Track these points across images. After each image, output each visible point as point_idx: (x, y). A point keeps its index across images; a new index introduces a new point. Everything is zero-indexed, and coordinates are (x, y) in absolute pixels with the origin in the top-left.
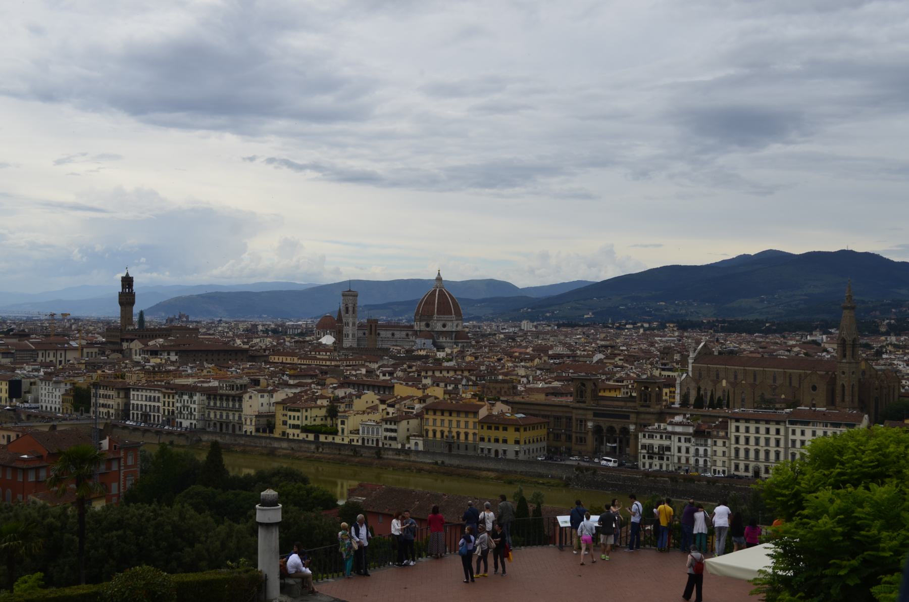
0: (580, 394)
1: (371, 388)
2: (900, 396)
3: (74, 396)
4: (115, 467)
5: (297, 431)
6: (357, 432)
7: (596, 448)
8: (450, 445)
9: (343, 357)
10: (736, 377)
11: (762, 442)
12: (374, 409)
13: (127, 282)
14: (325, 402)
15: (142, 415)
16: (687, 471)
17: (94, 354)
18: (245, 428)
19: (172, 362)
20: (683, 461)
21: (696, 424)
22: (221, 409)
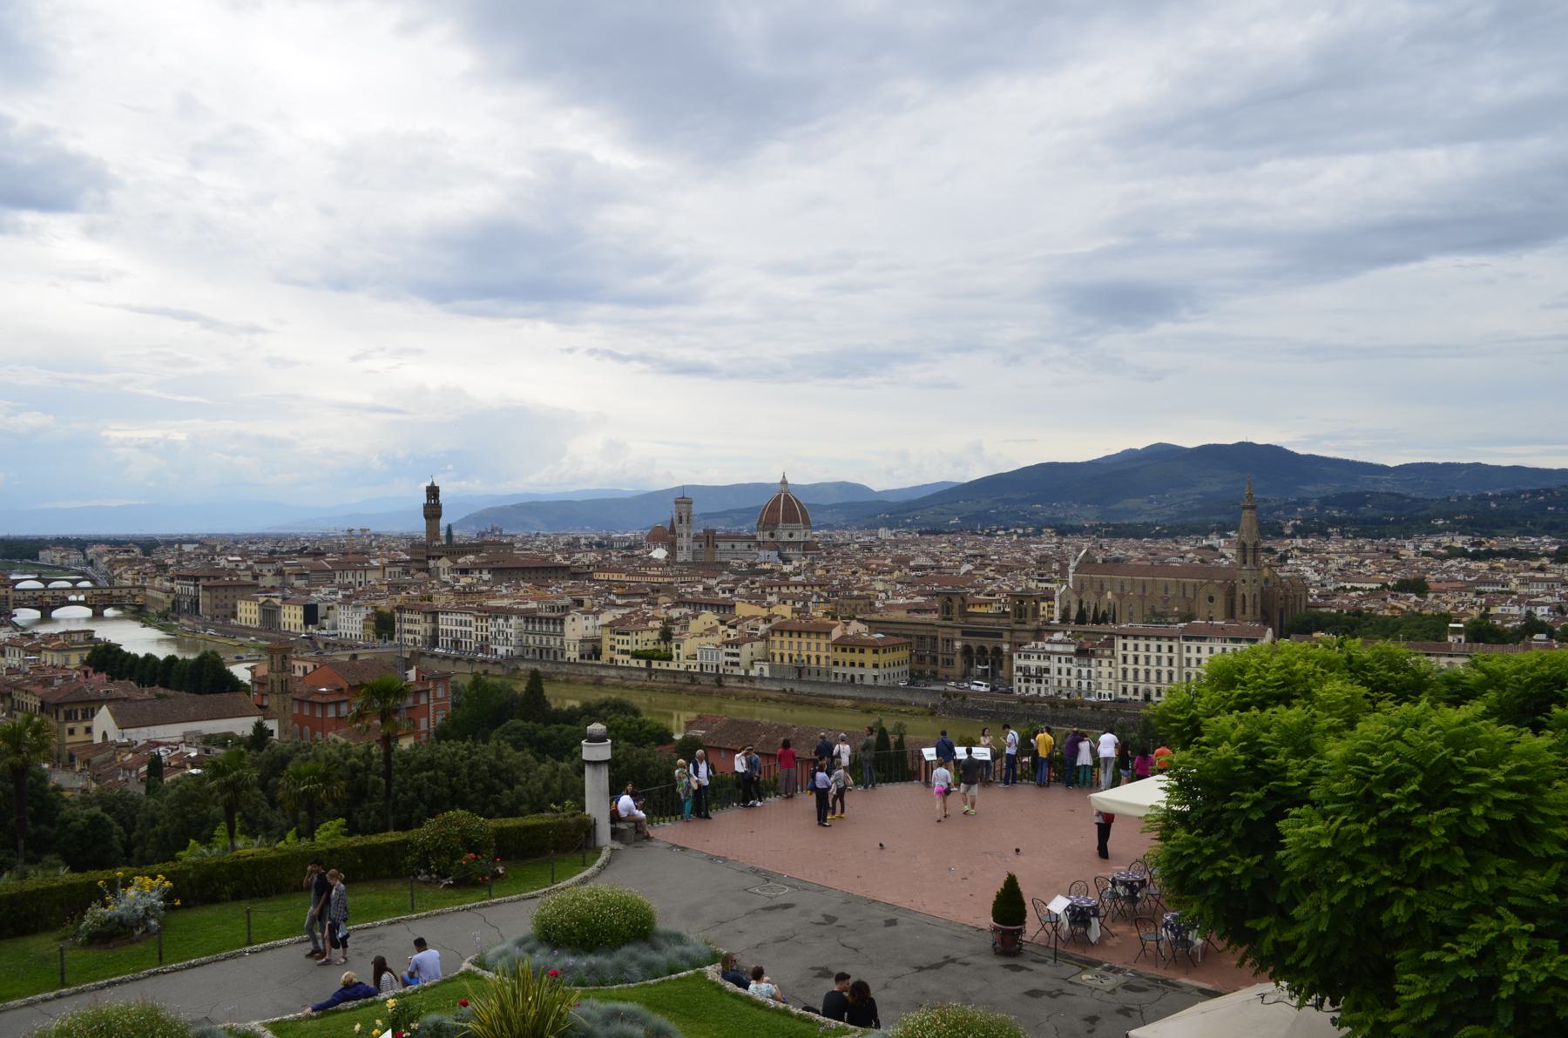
0: (947, 610)
2: (1307, 607)
3: (376, 622)
4: (423, 700)
5: (627, 657)
8: (800, 671)
10: (1122, 588)
11: (1153, 661)
12: (713, 630)
13: (433, 492)
14: (658, 624)
16: (1068, 695)
18: (567, 655)
19: (484, 581)
20: (1064, 684)
21: (1078, 643)
22: (541, 633)
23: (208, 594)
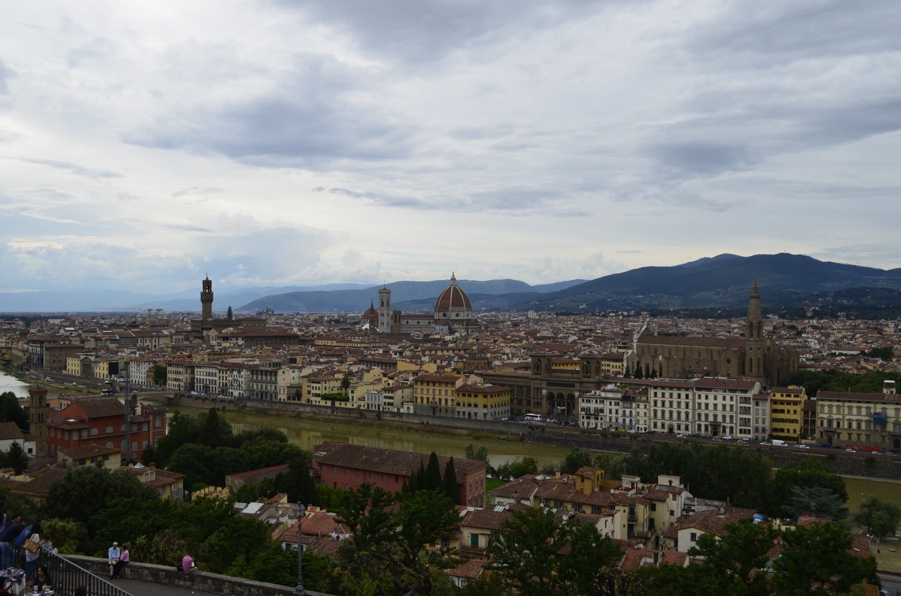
1: (380, 365)
2: (798, 367)
3: (154, 373)
4: (145, 428)
5: (318, 399)
6: (363, 399)
7: (550, 411)
8: (434, 409)
9: (372, 340)
10: (670, 353)
11: (675, 405)
13: (207, 284)
14: (341, 376)
15: (203, 387)
16: (616, 428)
17: (181, 340)
18: (279, 396)
20: (614, 420)
21: (624, 391)
22: (262, 382)
23: (48, 353)
